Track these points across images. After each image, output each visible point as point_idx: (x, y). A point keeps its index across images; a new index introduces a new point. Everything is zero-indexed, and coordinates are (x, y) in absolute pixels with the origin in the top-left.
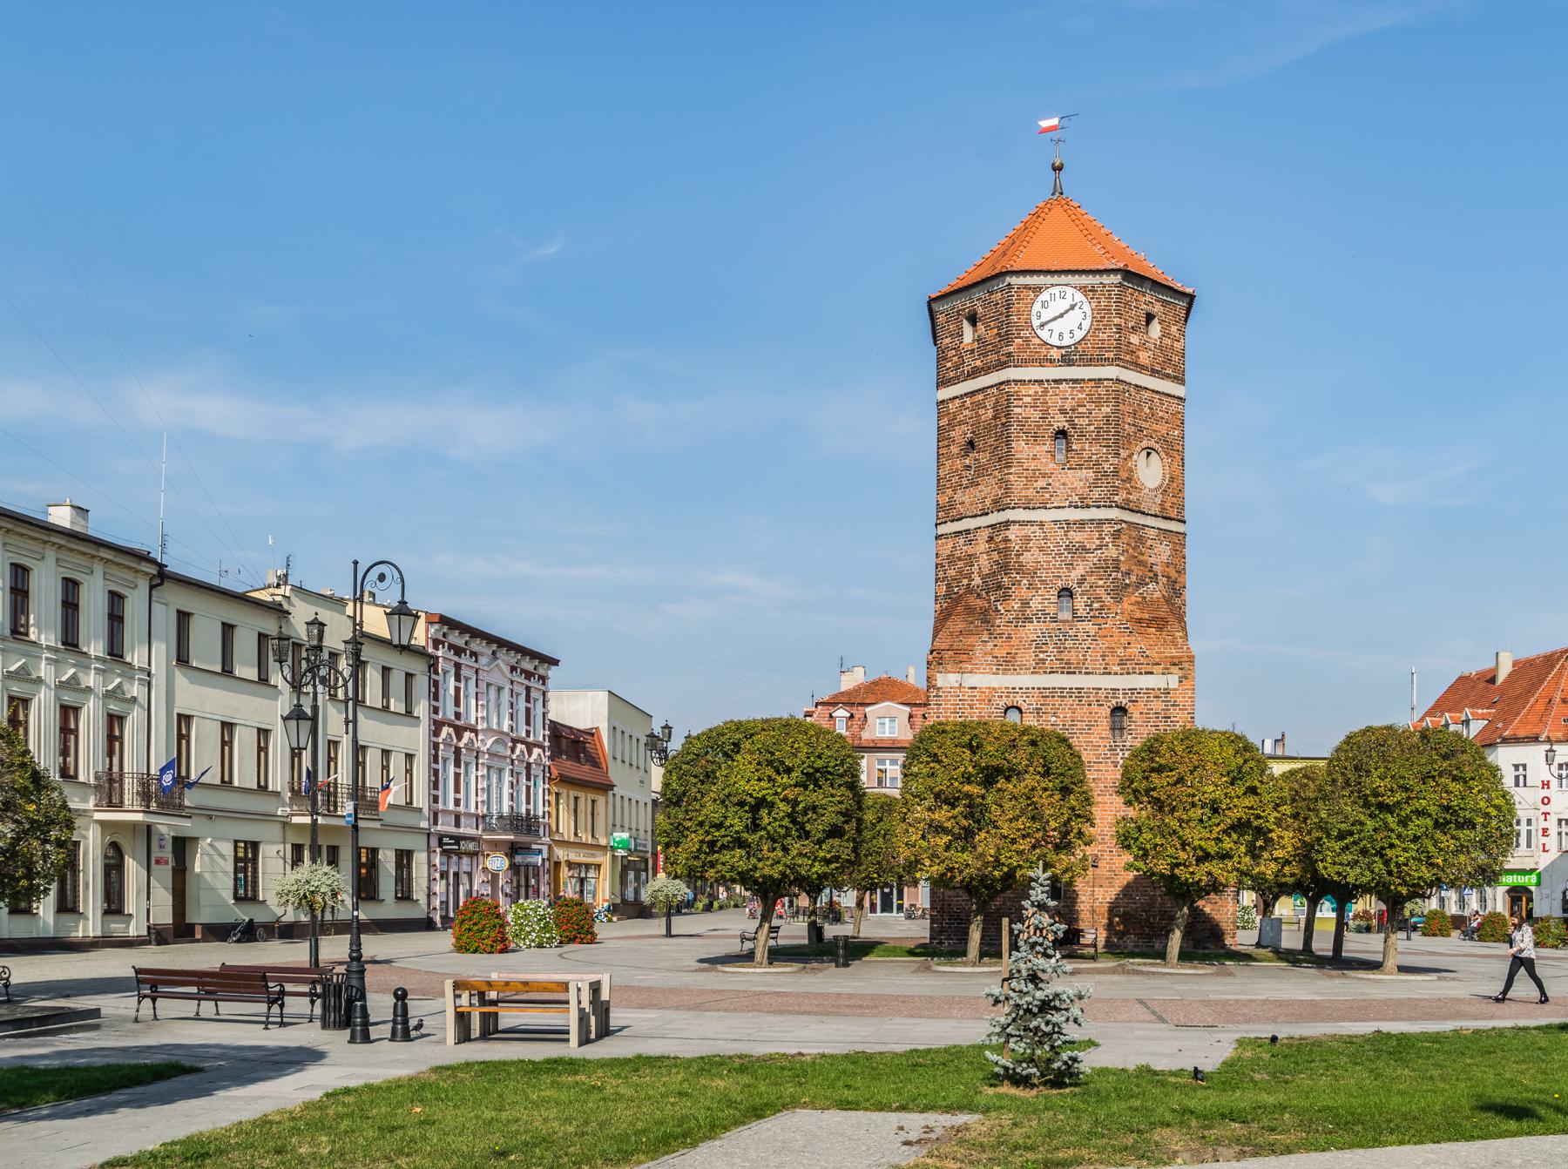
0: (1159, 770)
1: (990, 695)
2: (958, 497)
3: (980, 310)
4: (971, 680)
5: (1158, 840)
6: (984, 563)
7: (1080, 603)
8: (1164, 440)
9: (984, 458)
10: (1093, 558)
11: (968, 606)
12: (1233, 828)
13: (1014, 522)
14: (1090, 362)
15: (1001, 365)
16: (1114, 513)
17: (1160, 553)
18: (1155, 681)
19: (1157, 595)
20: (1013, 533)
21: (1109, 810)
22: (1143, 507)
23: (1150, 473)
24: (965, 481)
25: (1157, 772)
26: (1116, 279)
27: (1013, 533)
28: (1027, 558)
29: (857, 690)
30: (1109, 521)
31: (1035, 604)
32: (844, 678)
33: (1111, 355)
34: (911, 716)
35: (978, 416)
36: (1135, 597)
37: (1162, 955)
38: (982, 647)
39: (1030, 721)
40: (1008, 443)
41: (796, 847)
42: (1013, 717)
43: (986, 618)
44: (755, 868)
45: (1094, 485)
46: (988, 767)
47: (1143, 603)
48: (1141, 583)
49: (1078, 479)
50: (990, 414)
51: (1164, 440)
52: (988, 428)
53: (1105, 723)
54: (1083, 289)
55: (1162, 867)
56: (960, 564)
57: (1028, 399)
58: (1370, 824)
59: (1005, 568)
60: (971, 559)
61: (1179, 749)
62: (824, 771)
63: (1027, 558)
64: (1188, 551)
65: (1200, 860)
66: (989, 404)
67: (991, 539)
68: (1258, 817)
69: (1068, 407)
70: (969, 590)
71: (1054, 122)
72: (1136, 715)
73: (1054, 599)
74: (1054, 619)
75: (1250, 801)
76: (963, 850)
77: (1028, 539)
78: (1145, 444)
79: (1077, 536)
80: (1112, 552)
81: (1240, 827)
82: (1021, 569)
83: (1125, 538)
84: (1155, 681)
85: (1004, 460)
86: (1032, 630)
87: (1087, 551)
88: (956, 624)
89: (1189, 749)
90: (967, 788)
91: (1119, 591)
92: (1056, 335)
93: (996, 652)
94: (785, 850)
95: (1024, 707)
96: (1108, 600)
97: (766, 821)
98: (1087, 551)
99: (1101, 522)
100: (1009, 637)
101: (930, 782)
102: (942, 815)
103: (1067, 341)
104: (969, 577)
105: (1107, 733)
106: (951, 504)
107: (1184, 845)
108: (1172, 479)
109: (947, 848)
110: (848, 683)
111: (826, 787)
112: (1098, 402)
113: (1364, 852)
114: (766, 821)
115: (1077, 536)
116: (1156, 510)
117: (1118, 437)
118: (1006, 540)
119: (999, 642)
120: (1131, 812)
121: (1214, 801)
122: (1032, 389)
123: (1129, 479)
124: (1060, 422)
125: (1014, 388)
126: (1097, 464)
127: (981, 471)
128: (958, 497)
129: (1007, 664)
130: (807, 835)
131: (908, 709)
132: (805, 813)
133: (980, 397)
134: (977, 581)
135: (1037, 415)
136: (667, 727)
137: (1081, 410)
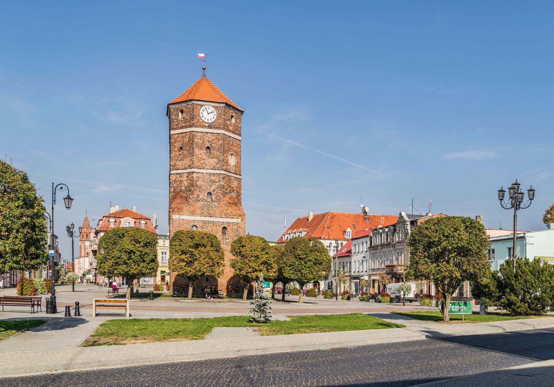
0: (243, 246)
1: (188, 222)
2: (177, 163)
4: (183, 217)
5: (243, 266)
6: (186, 183)
7: (213, 197)
8: (236, 152)
9: (185, 153)
10: (217, 184)
11: (180, 196)
12: (263, 263)
16: (223, 172)
17: (235, 184)
18: (234, 220)
19: (234, 196)
20: (195, 175)
21: (229, 257)
22: (230, 171)
23: (232, 161)
24: (179, 159)
25: (239, 246)
27: (195, 175)
28: (198, 183)
29: (117, 213)
30: (222, 174)
31: (201, 196)
32: (111, 208)
34: (135, 222)
36: (228, 196)
37: (241, 297)
38: (186, 208)
39: (200, 230)
41: (142, 265)
42: (194, 229)
43: (187, 199)
44: (130, 270)
45: (217, 163)
46: (191, 245)
47: (231, 198)
48: (230, 192)
49: (213, 161)
51: (236, 152)
53: (221, 232)
55: (244, 273)
56: (178, 183)
58: (297, 263)
59: (192, 185)
60: (181, 181)
61: (248, 241)
62: (149, 243)
63: (198, 183)
64: (242, 184)
65: (254, 272)
68: (269, 260)
70: (181, 191)
71: (203, 55)
72: (229, 230)
73: (206, 195)
74: (206, 201)
75: (267, 256)
76: (189, 267)
78: (231, 153)
79: (213, 178)
80: (222, 183)
81: (265, 263)
82: (197, 186)
83: (226, 179)
84: (234, 220)
85: (192, 154)
86: (200, 204)
87: (216, 182)
88: (178, 201)
89: (251, 241)
90: (190, 249)
91: (224, 194)
92: (210, 120)
93: (190, 209)
94: (139, 265)
95: (198, 226)
96: (221, 196)
97: (133, 257)
98: (216, 182)
99: (219, 174)
101: (180, 247)
102: (183, 257)
104: (181, 187)
105: (221, 234)
107: (250, 267)
108: (238, 163)
109: (185, 266)
110: (113, 210)
111: (149, 247)
113: (295, 270)
114: (133, 257)
115: (213, 178)
116: (234, 172)
117: (224, 150)
118: (192, 177)
119: (191, 207)
120: (233, 258)
121: (257, 256)
123: (227, 163)
125: (194, 133)
127: (185, 156)
128: (177, 163)
129: (193, 213)
130: (144, 261)
131: (134, 220)
132: (144, 255)
134: (183, 188)
136: (72, 224)
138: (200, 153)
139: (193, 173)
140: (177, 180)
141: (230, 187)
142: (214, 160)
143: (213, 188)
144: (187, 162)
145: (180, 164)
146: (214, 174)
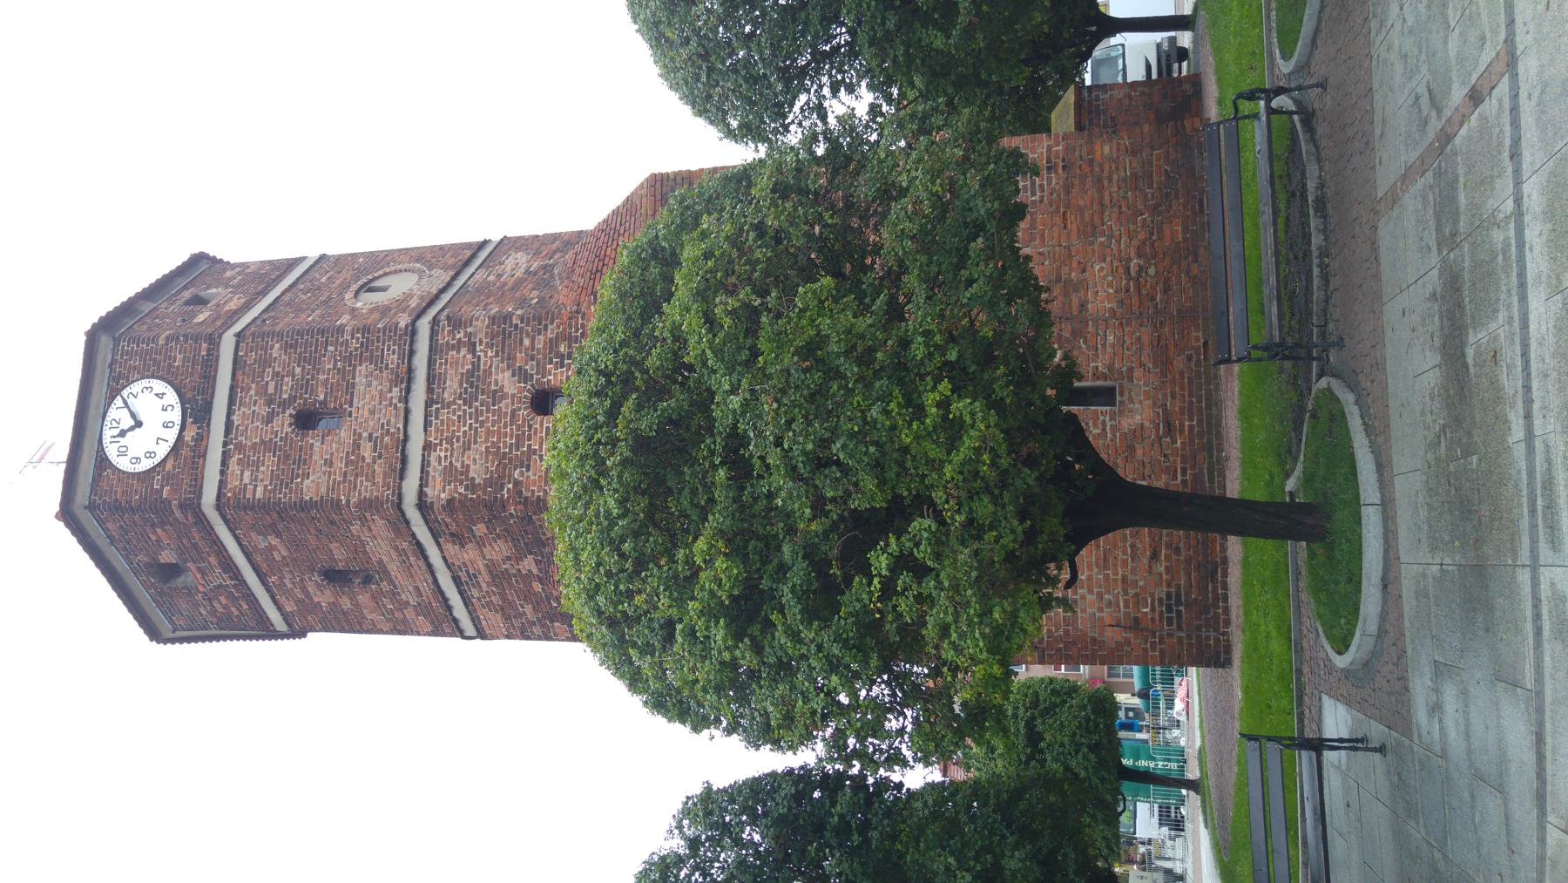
6: (499, 550)
10: (487, 356)
13: (421, 494)
14: (209, 378)
23: (400, 285)
24: (385, 586)
26: (105, 341)
28: (477, 473)
33: (204, 345)
40: (304, 506)
45: (378, 361)
52: (296, 544)
54: (113, 393)
56: (511, 595)
57: (247, 474)
59: (493, 509)
63: (477, 473)
67: (459, 539)
69: (264, 411)
77: (450, 474)
78: (349, 295)
79: (452, 386)
82: (496, 482)
87: (476, 366)
98: (476, 366)
99: (433, 349)
103: (176, 416)
106: (424, 609)
112: (266, 362)
115: (452, 386)
124: (283, 424)
126: (348, 359)
133: (258, 558)
134: (529, 564)
135: (270, 461)
137: (271, 390)
139: (423, 505)
141: (519, 283)
142: (360, 380)
143: (506, 380)
144: (380, 545)
146: (431, 379)
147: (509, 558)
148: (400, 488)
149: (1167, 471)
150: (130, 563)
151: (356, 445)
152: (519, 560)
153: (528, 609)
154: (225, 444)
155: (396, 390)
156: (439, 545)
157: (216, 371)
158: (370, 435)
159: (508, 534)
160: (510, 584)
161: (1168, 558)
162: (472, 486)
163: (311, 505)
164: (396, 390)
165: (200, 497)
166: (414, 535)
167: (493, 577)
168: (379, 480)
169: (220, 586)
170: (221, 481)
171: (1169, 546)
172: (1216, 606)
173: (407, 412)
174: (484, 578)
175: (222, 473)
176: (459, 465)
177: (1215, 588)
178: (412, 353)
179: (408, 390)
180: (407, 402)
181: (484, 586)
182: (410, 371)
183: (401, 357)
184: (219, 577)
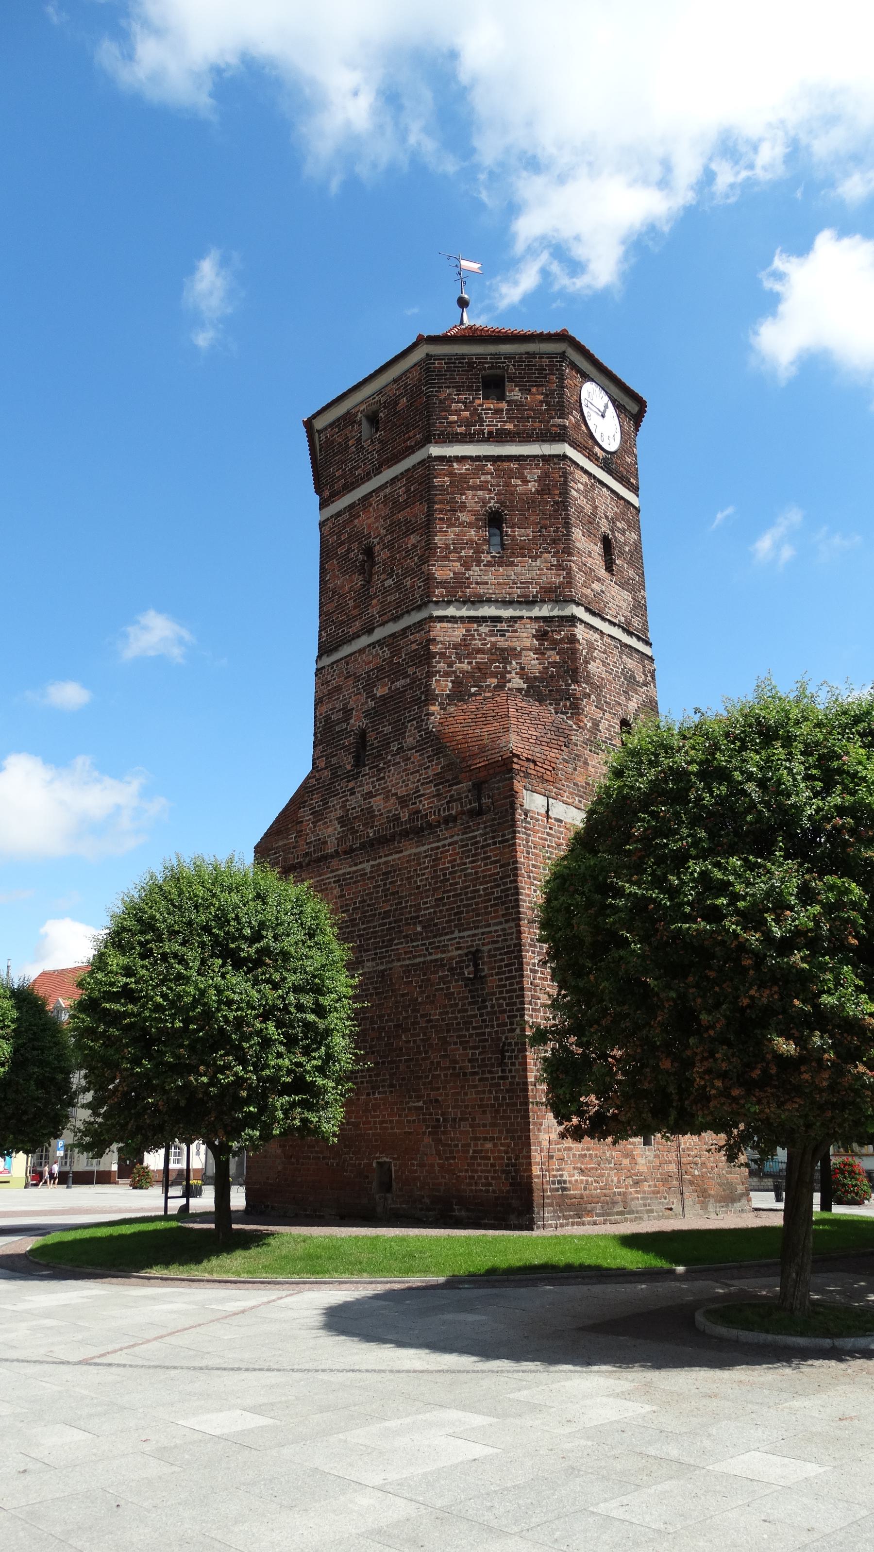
3: (512, 369)
6: (532, 663)
15: (560, 436)
24: (486, 558)
26: (634, 408)
27: (580, 631)
28: (593, 667)
35: (507, 484)
40: (567, 525)
50: (532, 486)
52: (530, 502)
54: (614, 401)
60: (505, 655)
63: (593, 667)
66: (533, 474)
67: (541, 636)
100: (586, 763)
118: (573, 639)
122: (585, 478)
124: (604, 527)
133: (513, 466)
134: (517, 682)
135: (588, 509)
138: (586, 548)
139: (573, 620)
140: (478, 643)
143: (633, 705)
144: (535, 571)
145: (489, 577)
147: (522, 669)
148: (582, 605)
149: (619, 1182)
150: (509, 357)
151: (599, 580)
152: (522, 673)
153: (465, 666)
154: (595, 477)
155: (623, 619)
156: (537, 619)
157: (624, 485)
158: (603, 592)
159: (545, 677)
160: (495, 661)
161: (582, 1181)
162: (587, 662)
163: (569, 534)
164: (623, 619)
165: (570, 445)
166: (543, 601)
167: (502, 650)
168: (585, 590)
169: (481, 421)
170: (578, 465)
171: (587, 1181)
172: (565, 1217)
173: (614, 624)
174: (502, 643)
175: (582, 468)
176: (595, 654)
177: (571, 1217)
178: (639, 638)
179: (624, 629)
180: (619, 626)
181: (493, 639)
182: (630, 634)
183: (637, 629)
184: (491, 424)
